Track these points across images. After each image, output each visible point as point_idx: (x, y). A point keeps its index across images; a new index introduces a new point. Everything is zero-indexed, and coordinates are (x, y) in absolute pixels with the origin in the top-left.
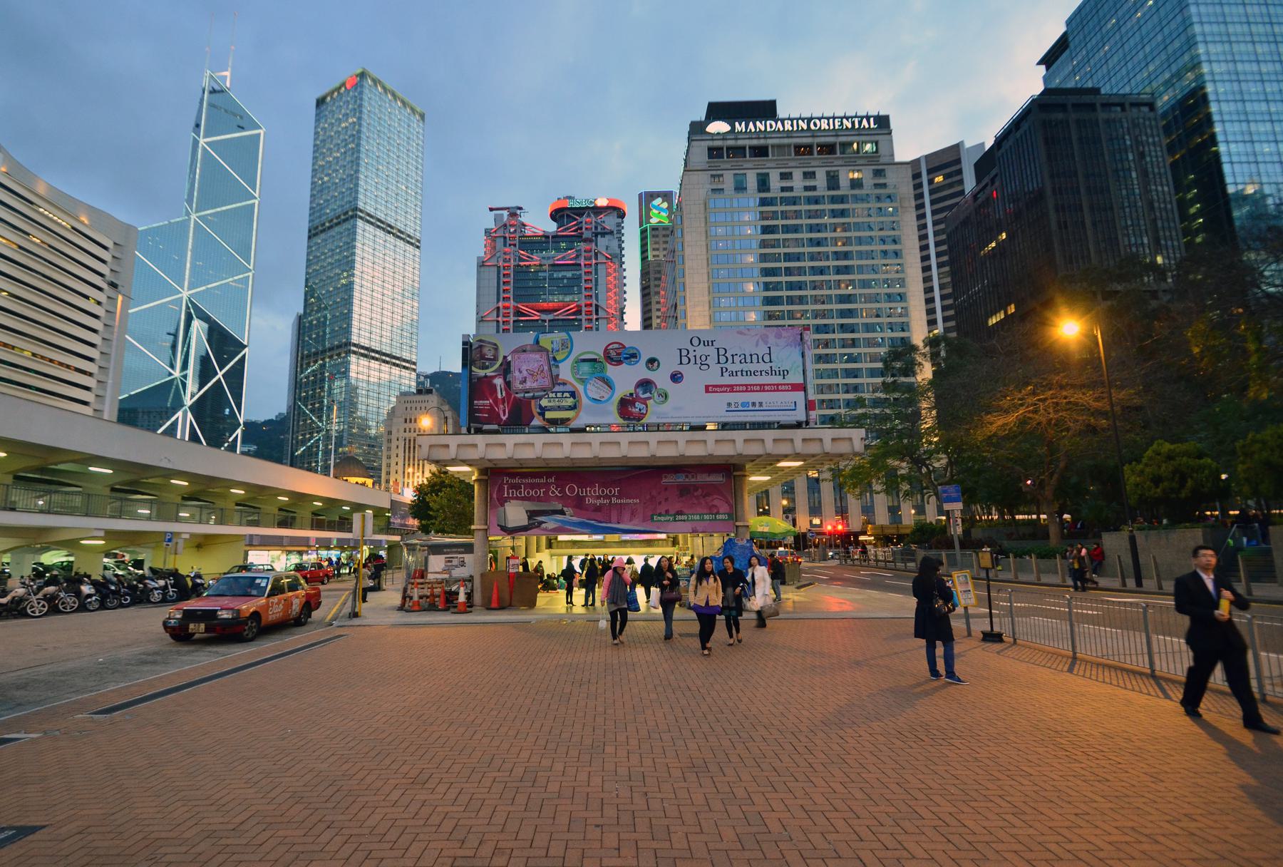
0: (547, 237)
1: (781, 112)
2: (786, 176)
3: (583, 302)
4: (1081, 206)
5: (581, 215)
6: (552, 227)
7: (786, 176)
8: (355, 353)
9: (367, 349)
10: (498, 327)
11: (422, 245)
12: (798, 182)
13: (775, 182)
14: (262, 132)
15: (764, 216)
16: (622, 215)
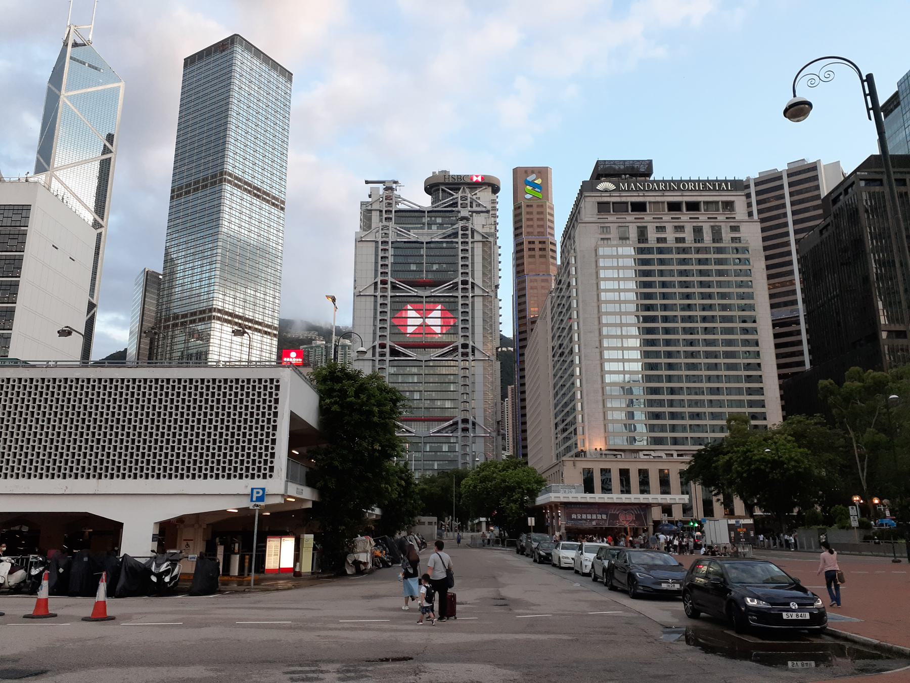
0: (424, 212)
1: (656, 175)
2: (661, 229)
3: (460, 279)
4: (894, 261)
5: (457, 190)
6: (425, 201)
7: (661, 229)
8: (219, 319)
9: (230, 314)
10: (376, 302)
11: (286, 207)
13: (652, 235)
14: (122, 85)
15: (646, 354)
16: (495, 189)
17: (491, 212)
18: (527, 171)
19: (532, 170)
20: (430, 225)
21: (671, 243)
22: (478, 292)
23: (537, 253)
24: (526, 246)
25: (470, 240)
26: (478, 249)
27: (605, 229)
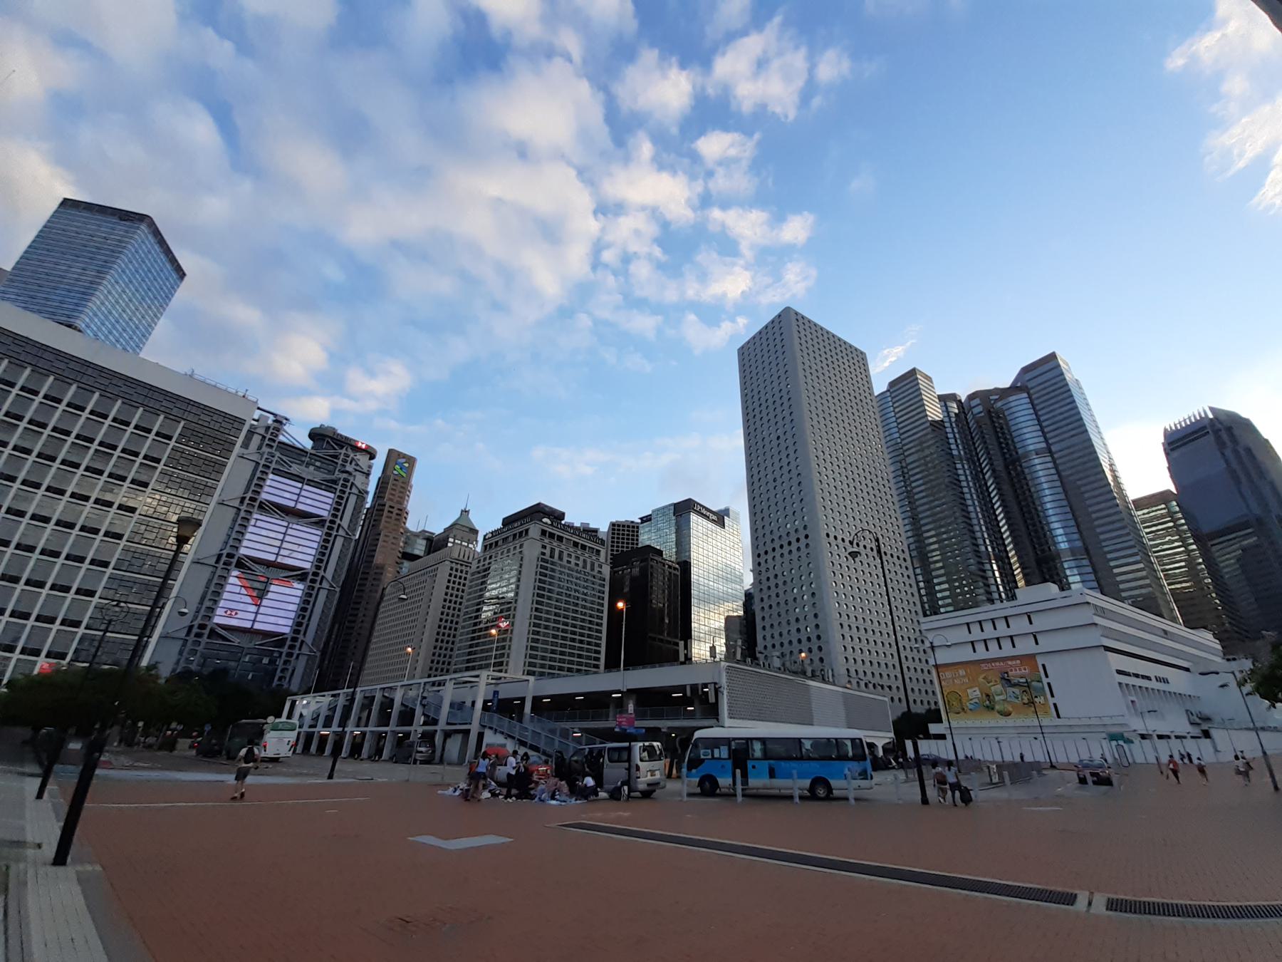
1: (567, 520)
2: (569, 556)
7: (569, 556)
12: (573, 560)
13: (565, 558)
16: (372, 457)
17: (368, 475)
18: (400, 455)
19: (404, 456)
20: (308, 465)
21: (572, 565)
22: (341, 532)
23: (394, 516)
24: (387, 508)
25: (348, 490)
26: (353, 499)
27: (544, 547)
